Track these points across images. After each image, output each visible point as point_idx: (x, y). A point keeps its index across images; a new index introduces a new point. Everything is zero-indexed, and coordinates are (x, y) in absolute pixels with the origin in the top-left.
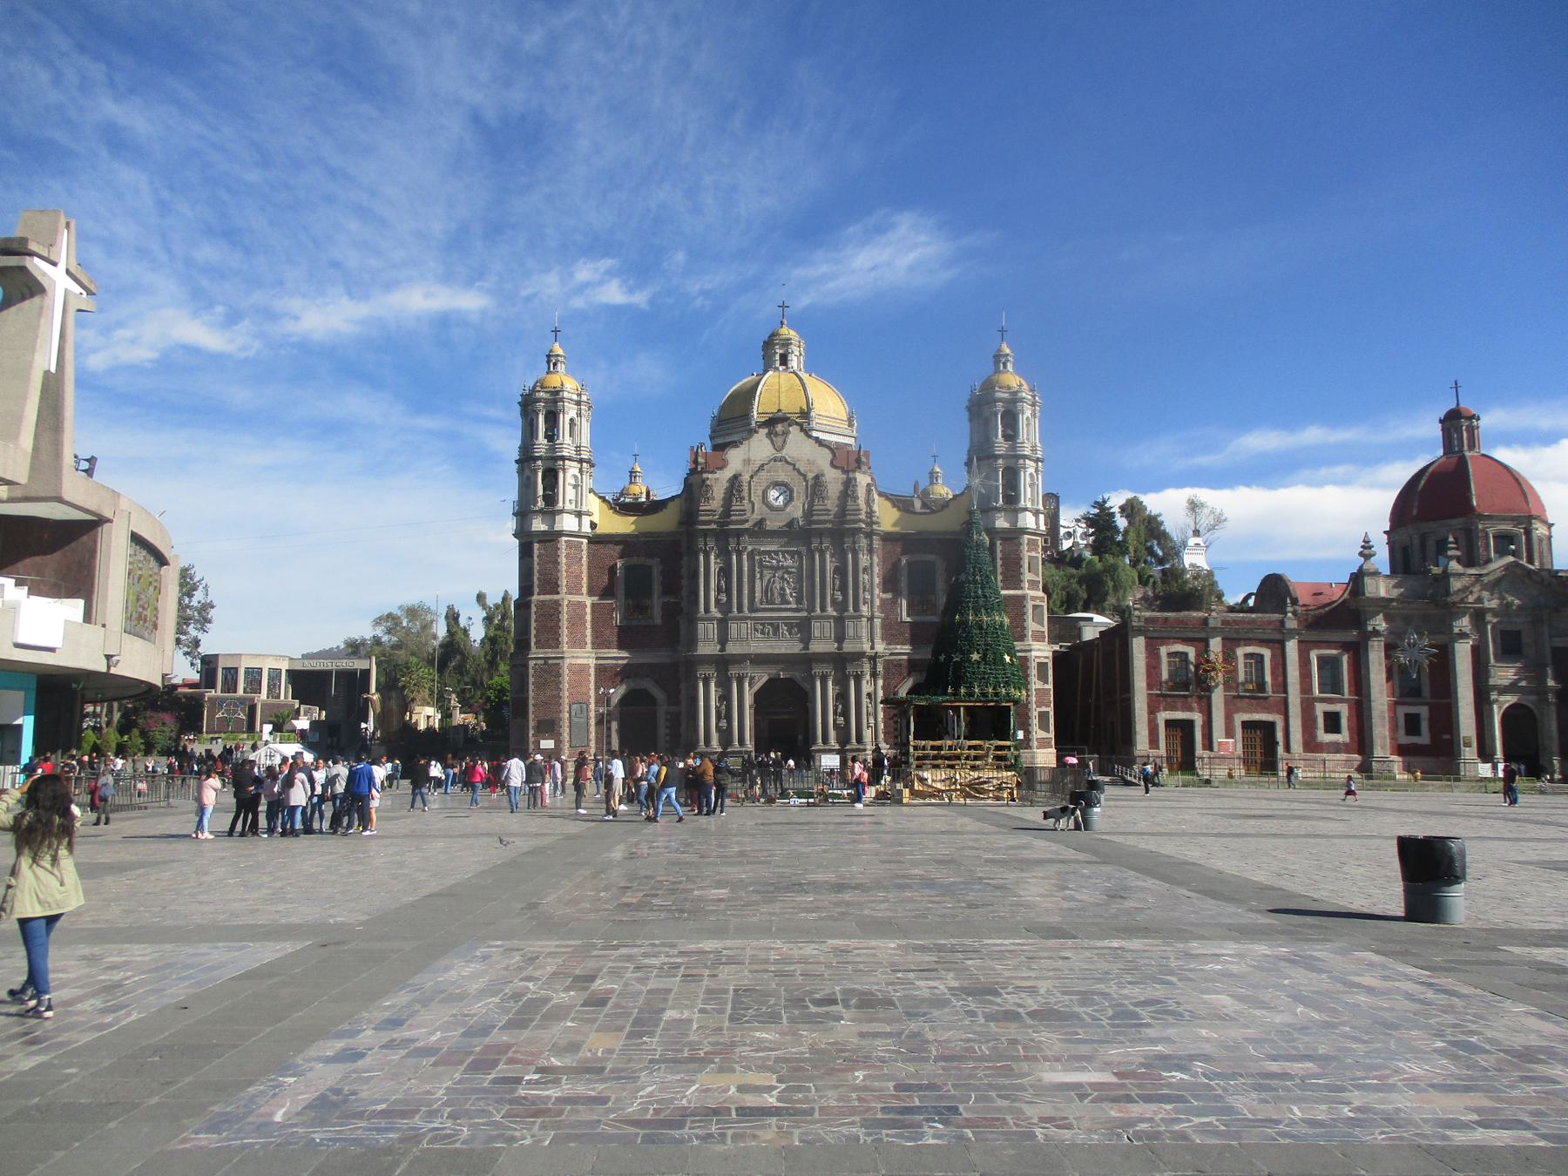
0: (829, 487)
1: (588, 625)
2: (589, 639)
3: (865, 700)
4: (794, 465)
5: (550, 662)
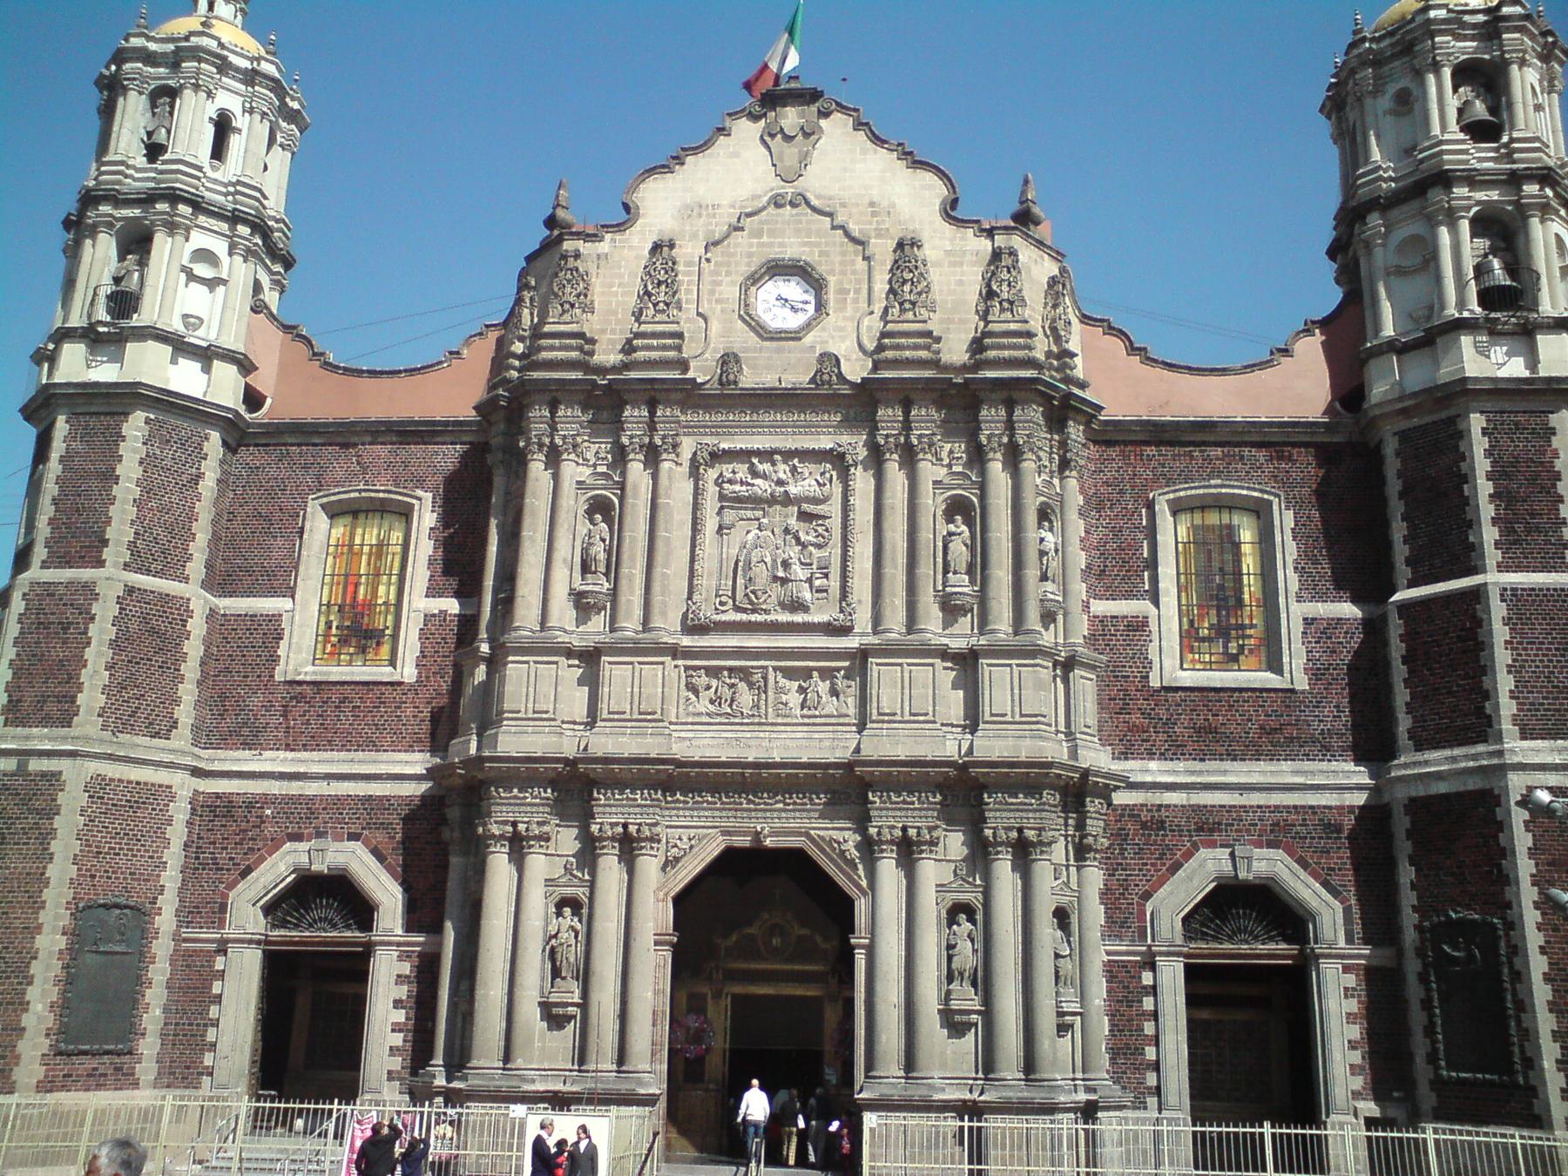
0: (934, 275)
1: (191, 669)
2: (185, 713)
3: (1047, 931)
4: (830, 215)
5: (35, 765)
